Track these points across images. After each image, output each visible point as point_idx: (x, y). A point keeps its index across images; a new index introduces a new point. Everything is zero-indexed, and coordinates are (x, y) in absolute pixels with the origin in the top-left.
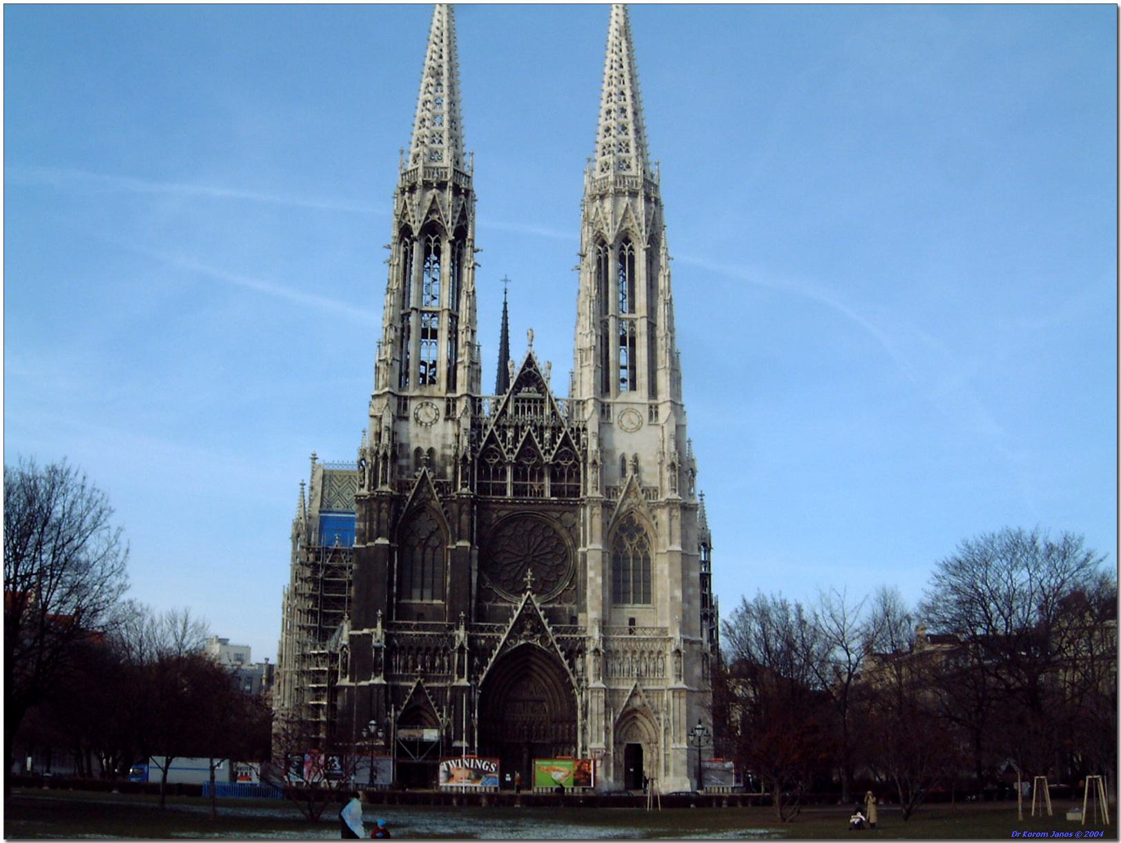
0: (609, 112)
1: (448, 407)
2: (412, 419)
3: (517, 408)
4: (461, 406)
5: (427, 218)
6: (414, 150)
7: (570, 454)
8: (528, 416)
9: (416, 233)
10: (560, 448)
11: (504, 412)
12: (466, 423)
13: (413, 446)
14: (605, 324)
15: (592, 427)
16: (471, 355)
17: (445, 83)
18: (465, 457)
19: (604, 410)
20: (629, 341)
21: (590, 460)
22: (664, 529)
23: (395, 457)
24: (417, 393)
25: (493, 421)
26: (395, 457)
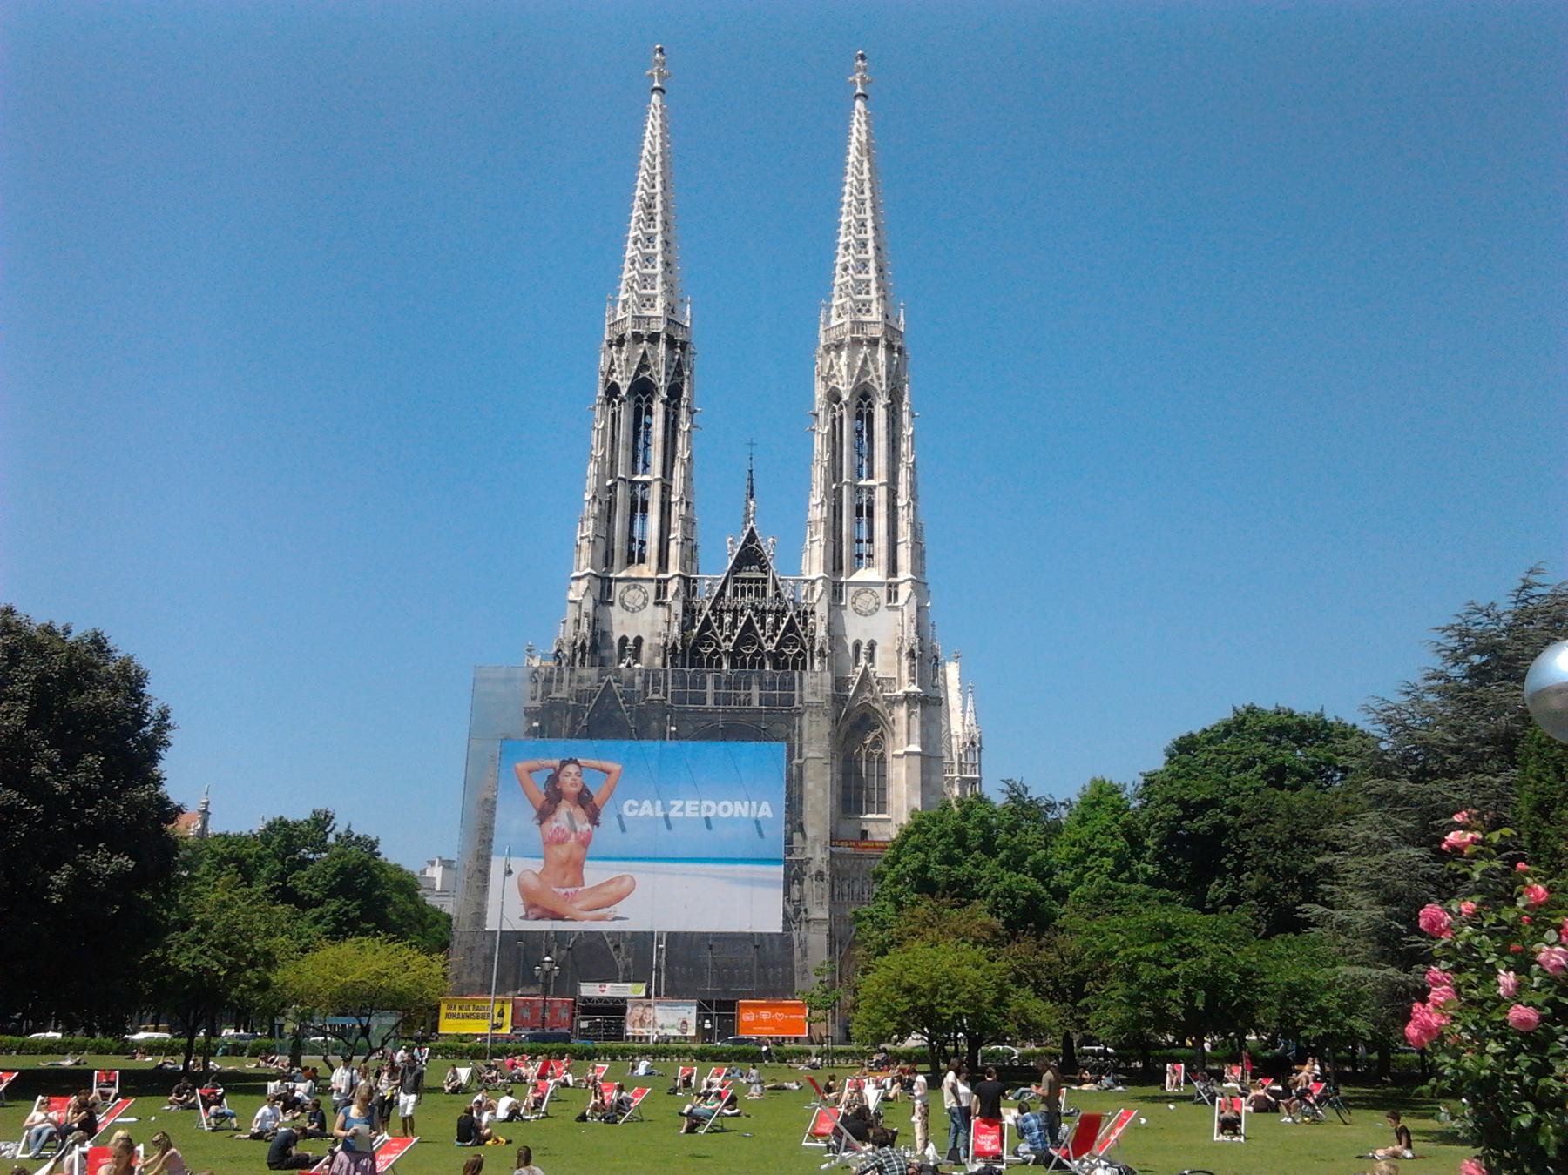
0: (847, 247)
1: (658, 589)
2: (617, 603)
3: (736, 589)
4: (672, 587)
5: (637, 375)
6: (623, 296)
7: (796, 642)
8: (749, 599)
9: (624, 392)
10: (784, 634)
11: (721, 593)
12: (678, 607)
14: (838, 492)
15: (821, 610)
16: (684, 530)
17: (658, 218)
18: (674, 646)
19: (836, 591)
20: (864, 511)
21: (817, 648)
22: (900, 728)
23: (595, 647)
24: (623, 574)
25: (708, 605)
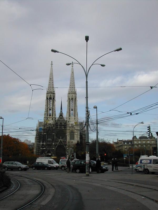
7: (66, 124)
12: (54, 121)
13: (49, 123)
26: (46, 124)
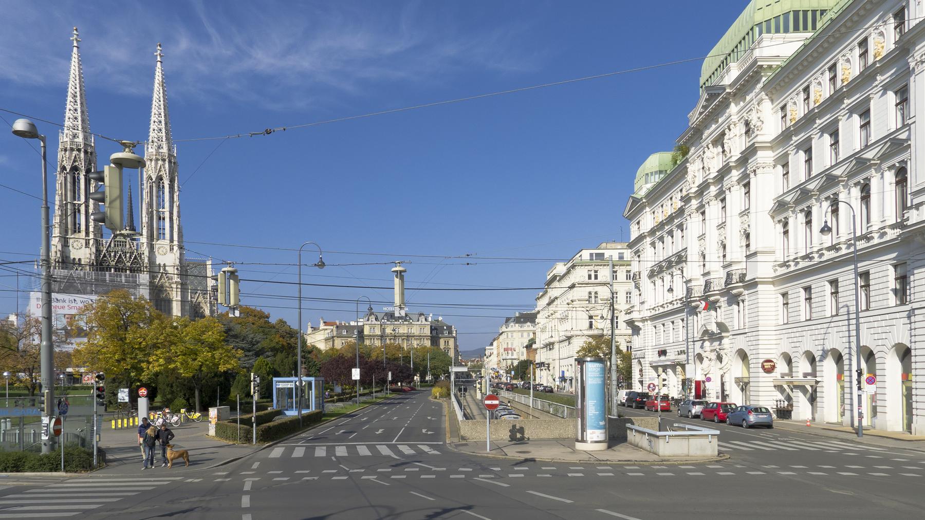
4: (91, 242)
11: (110, 246)
12: (94, 250)
15: (146, 253)
23: (63, 262)
